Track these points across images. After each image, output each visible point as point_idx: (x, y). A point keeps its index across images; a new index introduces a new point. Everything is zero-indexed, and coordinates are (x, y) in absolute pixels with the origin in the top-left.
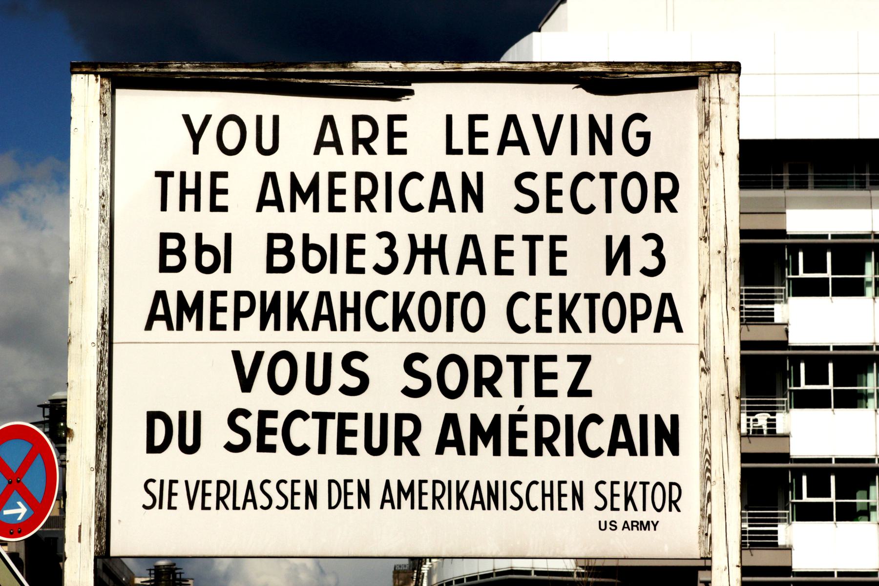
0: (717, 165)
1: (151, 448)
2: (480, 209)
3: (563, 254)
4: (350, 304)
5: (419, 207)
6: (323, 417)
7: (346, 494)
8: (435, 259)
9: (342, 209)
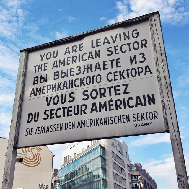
0: (156, 34)
1: (29, 122)
2: (99, 57)
3: (120, 62)
4: (71, 83)
5: (86, 60)
6: (64, 108)
7: (69, 125)
8: (89, 69)
9: (70, 64)
